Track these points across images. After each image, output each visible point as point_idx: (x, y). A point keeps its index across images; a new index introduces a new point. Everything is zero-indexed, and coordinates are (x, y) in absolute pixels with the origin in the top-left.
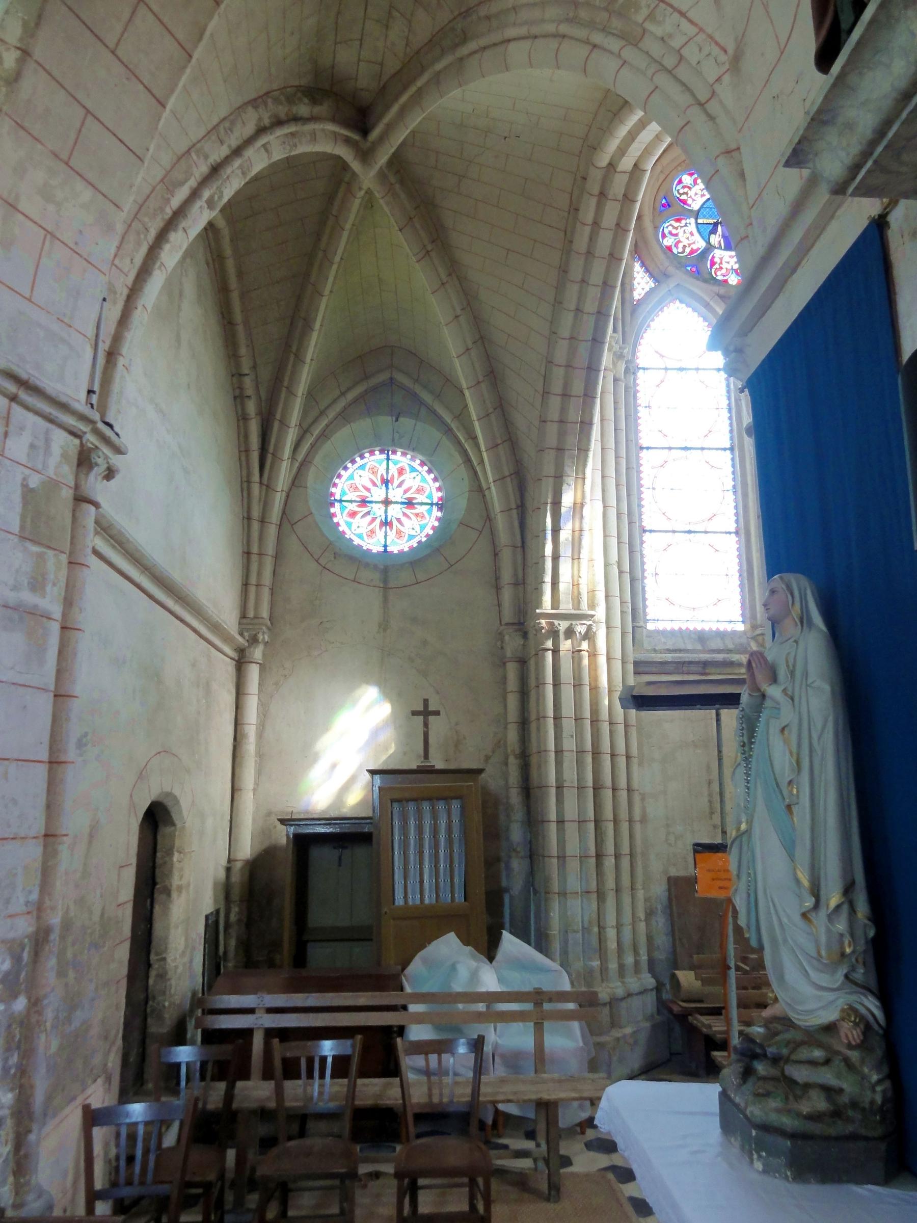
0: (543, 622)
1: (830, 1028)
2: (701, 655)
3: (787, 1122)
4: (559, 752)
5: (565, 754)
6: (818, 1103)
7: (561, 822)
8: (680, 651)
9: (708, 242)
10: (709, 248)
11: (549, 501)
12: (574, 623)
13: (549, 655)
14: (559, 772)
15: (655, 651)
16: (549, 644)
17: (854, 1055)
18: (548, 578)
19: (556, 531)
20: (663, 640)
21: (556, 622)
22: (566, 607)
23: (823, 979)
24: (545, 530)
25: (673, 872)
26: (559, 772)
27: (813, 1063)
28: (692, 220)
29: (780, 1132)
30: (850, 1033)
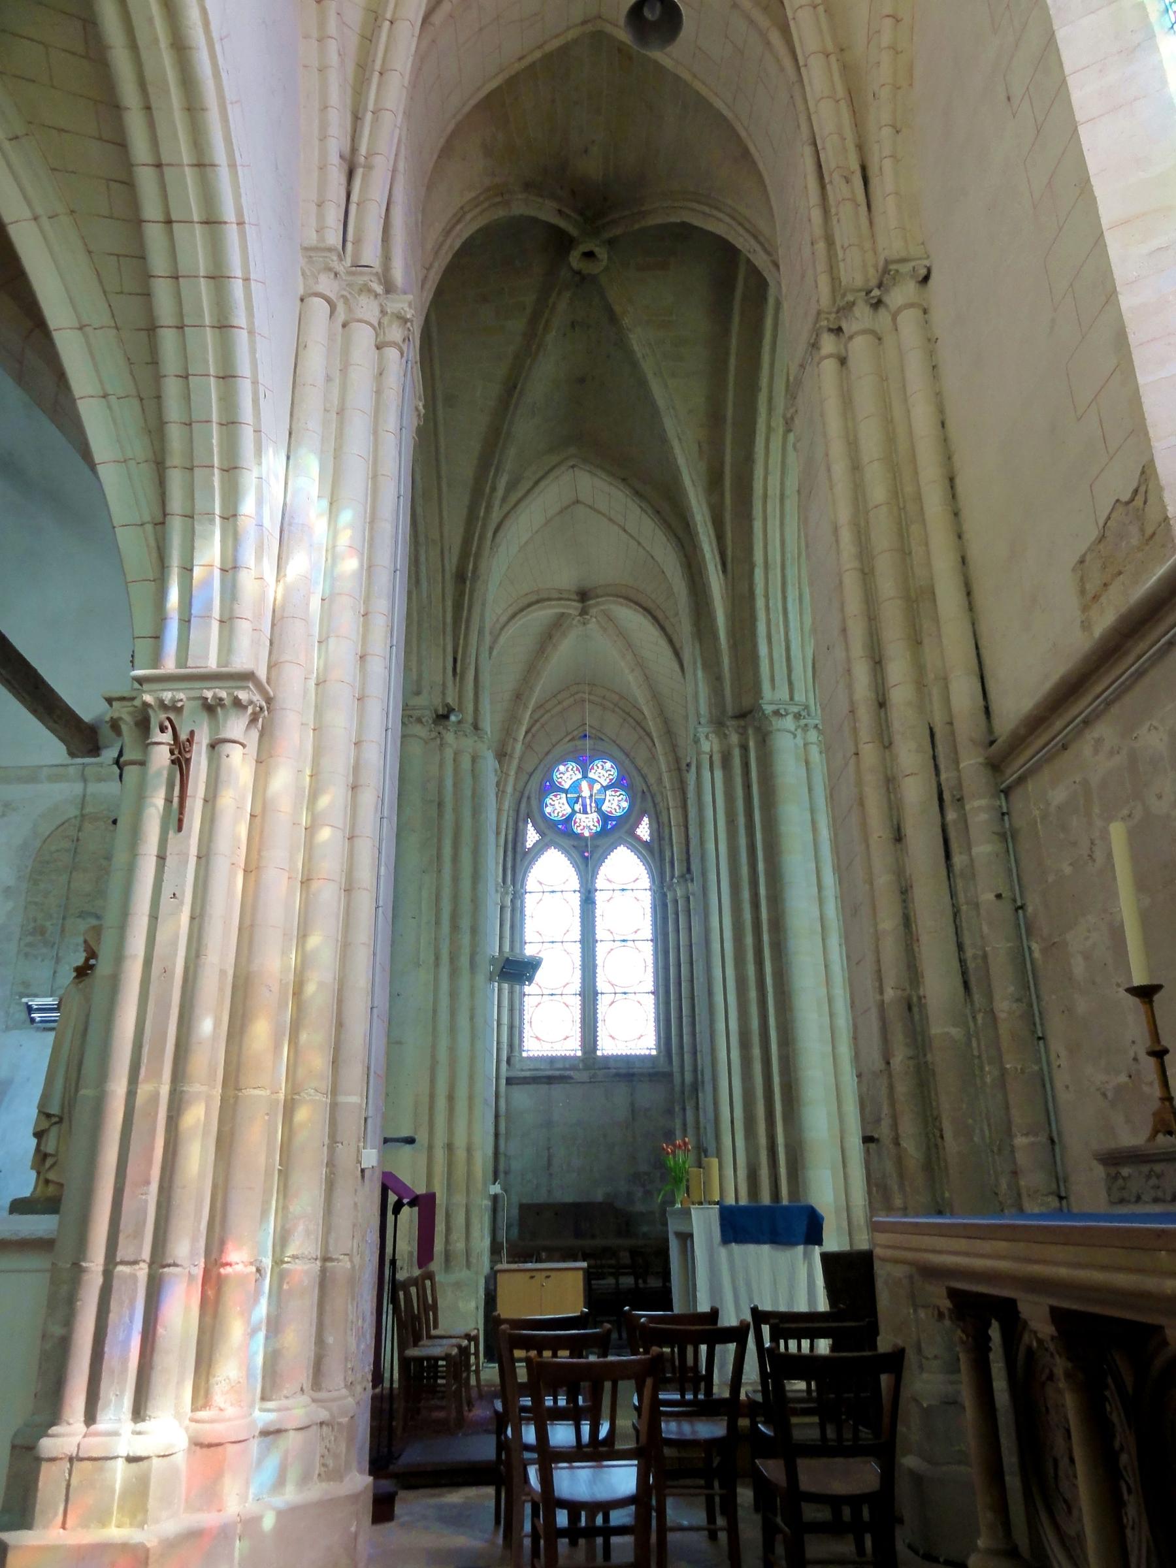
9: (573, 809)
10: (574, 812)
15: (522, 1070)
25: (524, 1201)
28: (564, 795)
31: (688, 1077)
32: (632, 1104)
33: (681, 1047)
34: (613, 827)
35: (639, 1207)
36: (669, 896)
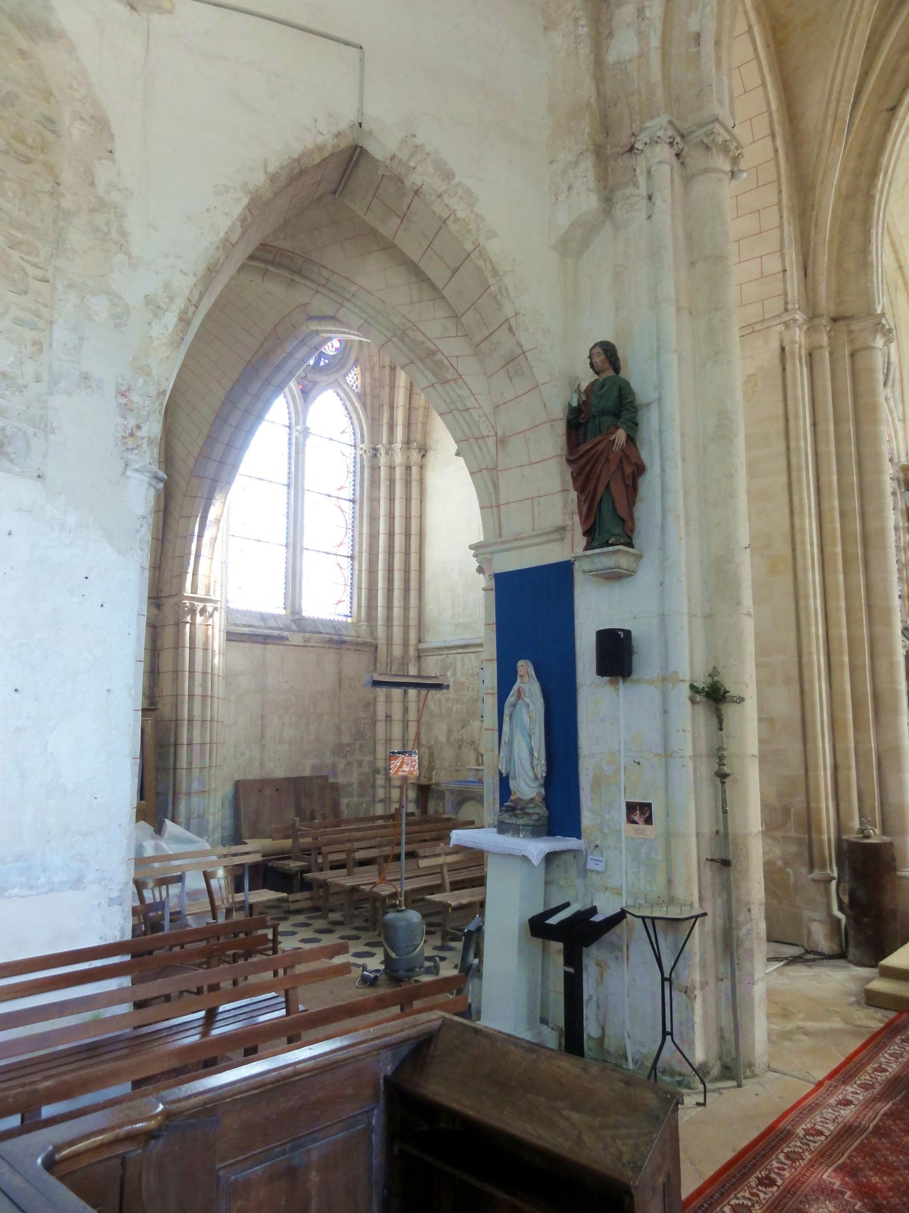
0: (187, 603)
1: (532, 799)
2: (265, 631)
3: (530, 823)
4: (191, 696)
5: (195, 697)
6: (535, 817)
7: (190, 744)
8: (251, 626)
11: (200, 515)
12: (207, 604)
13: (188, 626)
14: (190, 710)
15: (236, 625)
16: (188, 618)
17: (540, 804)
18: (190, 570)
19: (200, 536)
20: (240, 617)
21: (196, 603)
22: (201, 593)
23: (532, 785)
24: (193, 535)
26: (190, 710)
27: (532, 808)
29: (529, 825)
30: (539, 799)
31: (397, 651)
32: (340, 673)
33: (389, 618)
34: (326, 365)
35: (341, 780)
36: (383, 460)
